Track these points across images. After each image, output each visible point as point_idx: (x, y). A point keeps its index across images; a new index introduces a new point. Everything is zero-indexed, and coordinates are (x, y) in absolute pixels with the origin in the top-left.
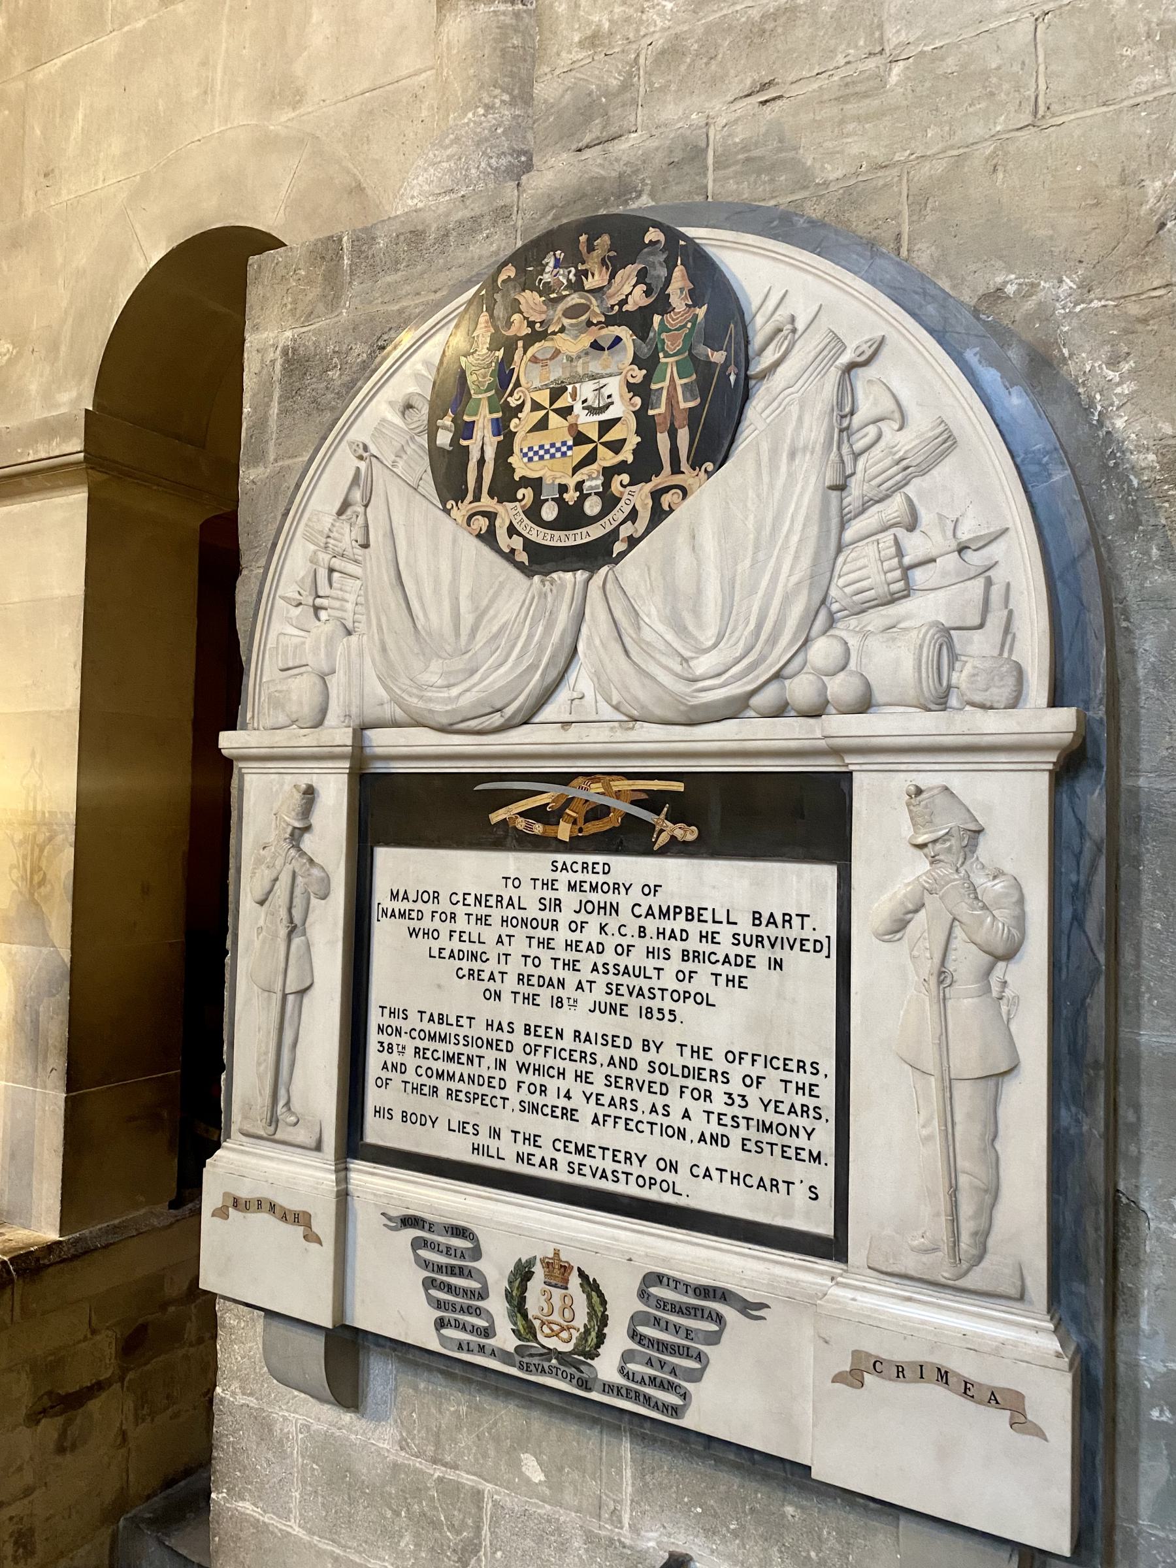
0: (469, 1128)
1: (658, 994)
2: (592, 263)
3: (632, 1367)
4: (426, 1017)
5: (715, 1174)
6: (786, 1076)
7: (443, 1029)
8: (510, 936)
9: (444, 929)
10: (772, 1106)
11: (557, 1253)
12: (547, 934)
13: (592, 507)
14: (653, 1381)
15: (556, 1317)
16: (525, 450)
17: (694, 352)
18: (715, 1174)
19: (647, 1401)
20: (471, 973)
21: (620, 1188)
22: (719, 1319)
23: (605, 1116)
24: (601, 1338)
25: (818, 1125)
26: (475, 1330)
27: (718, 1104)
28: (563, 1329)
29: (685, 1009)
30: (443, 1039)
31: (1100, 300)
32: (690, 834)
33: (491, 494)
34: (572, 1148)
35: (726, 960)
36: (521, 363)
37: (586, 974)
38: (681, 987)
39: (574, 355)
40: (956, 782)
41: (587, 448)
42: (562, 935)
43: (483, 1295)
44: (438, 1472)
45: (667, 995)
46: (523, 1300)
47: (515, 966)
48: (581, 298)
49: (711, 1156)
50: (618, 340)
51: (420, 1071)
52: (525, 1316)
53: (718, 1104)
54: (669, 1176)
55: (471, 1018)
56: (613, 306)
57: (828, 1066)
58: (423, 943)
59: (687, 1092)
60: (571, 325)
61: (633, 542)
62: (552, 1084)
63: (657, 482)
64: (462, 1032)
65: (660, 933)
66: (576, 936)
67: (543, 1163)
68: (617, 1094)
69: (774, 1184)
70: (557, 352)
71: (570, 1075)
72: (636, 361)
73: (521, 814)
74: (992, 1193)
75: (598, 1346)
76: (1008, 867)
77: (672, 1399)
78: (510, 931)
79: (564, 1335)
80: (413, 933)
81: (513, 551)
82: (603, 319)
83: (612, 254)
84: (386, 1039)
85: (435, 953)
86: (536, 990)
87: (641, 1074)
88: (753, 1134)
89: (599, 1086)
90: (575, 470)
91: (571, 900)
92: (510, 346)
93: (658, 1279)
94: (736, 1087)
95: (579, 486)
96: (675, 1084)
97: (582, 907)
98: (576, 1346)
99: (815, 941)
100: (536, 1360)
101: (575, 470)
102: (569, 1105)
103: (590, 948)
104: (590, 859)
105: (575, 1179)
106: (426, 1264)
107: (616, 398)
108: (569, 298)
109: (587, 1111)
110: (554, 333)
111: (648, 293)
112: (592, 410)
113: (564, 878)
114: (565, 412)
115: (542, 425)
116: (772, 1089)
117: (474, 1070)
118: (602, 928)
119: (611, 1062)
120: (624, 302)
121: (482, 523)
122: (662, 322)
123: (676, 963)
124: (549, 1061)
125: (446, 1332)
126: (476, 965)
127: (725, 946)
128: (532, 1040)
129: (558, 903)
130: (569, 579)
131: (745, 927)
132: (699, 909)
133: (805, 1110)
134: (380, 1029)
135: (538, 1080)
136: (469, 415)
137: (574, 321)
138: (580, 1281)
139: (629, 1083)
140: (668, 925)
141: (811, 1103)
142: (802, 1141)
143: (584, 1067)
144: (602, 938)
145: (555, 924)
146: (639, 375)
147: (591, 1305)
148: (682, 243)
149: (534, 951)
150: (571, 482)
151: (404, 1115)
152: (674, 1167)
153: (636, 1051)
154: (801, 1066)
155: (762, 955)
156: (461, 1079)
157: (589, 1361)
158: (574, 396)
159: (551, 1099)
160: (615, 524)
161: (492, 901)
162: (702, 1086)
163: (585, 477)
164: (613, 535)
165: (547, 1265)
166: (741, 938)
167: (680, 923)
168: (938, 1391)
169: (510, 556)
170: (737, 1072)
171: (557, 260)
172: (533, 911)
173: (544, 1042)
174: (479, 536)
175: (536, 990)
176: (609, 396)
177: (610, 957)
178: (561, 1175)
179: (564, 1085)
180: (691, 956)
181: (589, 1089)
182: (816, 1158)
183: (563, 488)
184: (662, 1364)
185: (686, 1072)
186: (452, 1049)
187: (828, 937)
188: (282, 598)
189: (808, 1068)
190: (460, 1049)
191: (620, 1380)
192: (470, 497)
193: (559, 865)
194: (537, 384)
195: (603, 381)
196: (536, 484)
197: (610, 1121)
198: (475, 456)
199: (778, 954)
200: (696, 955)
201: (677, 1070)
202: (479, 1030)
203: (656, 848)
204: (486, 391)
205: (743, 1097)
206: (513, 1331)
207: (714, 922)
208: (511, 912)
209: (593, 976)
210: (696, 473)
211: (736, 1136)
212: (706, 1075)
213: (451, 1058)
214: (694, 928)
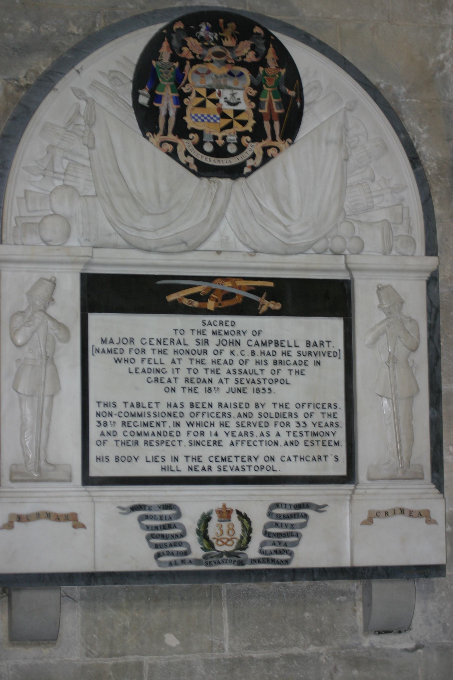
0: (159, 459)
1: (262, 381)
2: (227, 33)
3: (265, 548)
4: (128, 405)
5: (293, 459)
6: (323, 411)
7: (140, 410)
8: (179, 359)
9: (138, 358)
10: (317, 425)
11: (224, 506)
12: (202, 357)
13: (232, 149)
14: (276, 552)
15: (225, 535)
16: (193, 115)
17: (280, 88)
18: (293, 459)
19: (274, 561)
20: (156, 380)
21: (247, 473)
22: (306, 516)
23: (236, 441)
24: (249, 539)
25: (337, 429)
26: (179, 554)
27: (293, 427)
28: (229, 540)
29: (276, 387)
30: (140, 415)
31: (415, 99)
32: (277, 306)
33: (174, 133)
34: (219, 459)
35: (295, 363)
36: (189, 71)
37: (224, 374)
38: (273, 377)
39: (219, 76)
40: (394, 284)
41: (227, 121)
42: (210, 357)
43: (183, 535)
44: (111, 662)
45: (267, 382)
46: (206, 532)
47: (183, 374)
48: (221, 48)
49: (291, 451)
50: (241, 74)
51: (126, 434)
52: (207, 538)
53: (293, 427)
54: (270, 463)
55: (157, 403)
56: (238, 58)
57: (342, 404)
58: (124, 367)
59: (278, 424)
60: (217, 61)
61: (254, 169)
62: (207, 431)
63: (264, 143)
64: (152, 411)
65: (262, 353)
66: (218, 357)
67: (204, 469)
68: (243, 430)
69: (320, 458)
70: (209, 72)
71: (217, 424)
72: (252, 85)
73: (187, 297)
74: (412, 440)
75: (247, 543)
76: (414, 317)
77: (285, 557)
78: (179, 356)
79: (230, 543)
80: (118, 361)
81: (188, 164)
82: (233, 62)
83: (237, 32)
84: (102, 419)
85: (133, 370)
86: (196, 385)
87: (255, 419)
88: (310, 438)
89: (233, 426)
90: (222, 130)
91: (214, 340)
92: (183, 62)
93: (277, 505)
94: (301, 419)
95: (224, 138)
96: (271, 422)
97: (220, 342)
98: (236, 546)
99: (334, 352)
100: (214, 559)
101: (222, 130)
102: (217, 439)
103: (226, 362)
104: (224, 318)
105: (223, 474)
106: (148, 528)
107: (242, 100)
108: (215, 47)
109: (227, 440)
110: (207, 62)
111: (257, 56)
112: (230, 104)
113: (209, 329)
114: (215, 101)
115: (202, 105)
116: (317, 417)
117: (161, 429)
118: (232, 353)
119: (239, 415)
120: (244, 57)
121: (170, 148)
122: (264, 72)
123: (271, 366)
124: (205, 419)
125: (162, 559)
126: (159, 376)
127: (294, 357)
128: (195, 410)
129: (207, 342)
130: (226, 182)
131: (303, 348)
132: (281, 341)
133: (332, 424)
134: (98, 414)
135: (199, 429)
136: (159, 91)
137: (218, 59)
138: (237, 515)
139: (249, 424)
140: (266, 349)
141: (334, 420)
142: (331, 438)
143: (224, 420)
144: (232, 357)
145: (205, 352)
146: (253, 93)
147: (243, 525)
148: (272, 37)
149: (194, 366)
150: (220, 135)
151: (117, 459)
152: (273, 459)
153: (252, 409)
154: (330, 406)
155: (311, 360)
156: (153, 434)
157: (243, 551)
158: (219, 94)
159: (207, 437)
160: (244, 159)
161: (168, 342)
162: (285, 420)
163: (227, 134)
164: (243, 164)
165: (219, 512)
166: (301, 353)
167: (272, 348)
168: (400, 518)
169: (187, 166)
170: (301, 412)
171: (207, 27)
172: (192, 345)
173: (202, 410)
174: (168, 153)
175: (196, 385)
176: (239, 99)
177: (236, 366)
178: (215, 473)
179: (213, 430)
180: (278, 362)
181: (227, 430)
182: (337, 444)
183: (215, 138)
184: (280, 543)
185: (278, 415)
186: (146, 420)
187: (340, 350)
188: (24, 168)
189: (333, 406)
190: (152, 419)
191: (258, 556)
192: (161, 132)
193: (207, 323)
194: (198, 84)
195: (235, 91)
196: (201, 133)
197: (240, 443)
198: (163, 113)
199: (318, 358)
200: (281, 362)
201: (273, 415)
202: (163, 408)
203: (260, 312)
204: (170, 81)
205: (304, 423)
206: (202, 548)
207: (289, 346)
208: (179, 347)
209: (228, 376)
210: (283, 142)
211: (301, 440)
212: (287, 415)
213: (145, 425)
214: (279, 350)
